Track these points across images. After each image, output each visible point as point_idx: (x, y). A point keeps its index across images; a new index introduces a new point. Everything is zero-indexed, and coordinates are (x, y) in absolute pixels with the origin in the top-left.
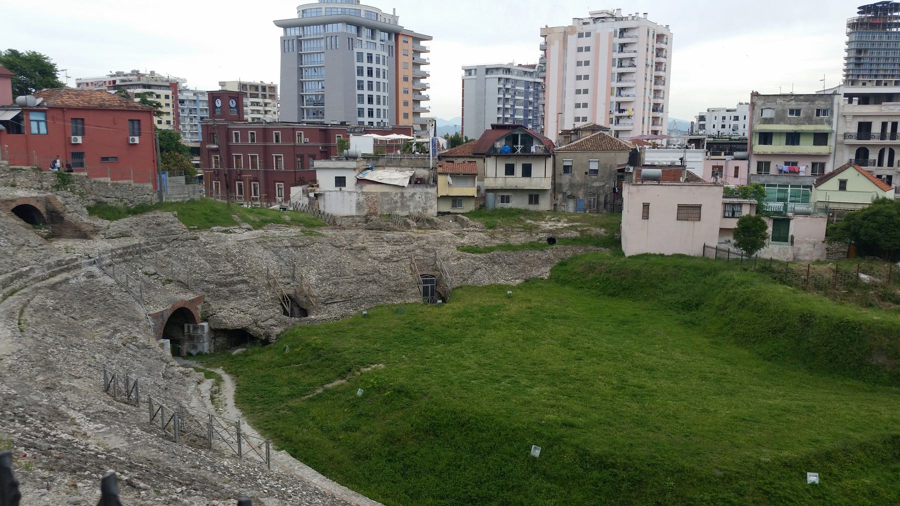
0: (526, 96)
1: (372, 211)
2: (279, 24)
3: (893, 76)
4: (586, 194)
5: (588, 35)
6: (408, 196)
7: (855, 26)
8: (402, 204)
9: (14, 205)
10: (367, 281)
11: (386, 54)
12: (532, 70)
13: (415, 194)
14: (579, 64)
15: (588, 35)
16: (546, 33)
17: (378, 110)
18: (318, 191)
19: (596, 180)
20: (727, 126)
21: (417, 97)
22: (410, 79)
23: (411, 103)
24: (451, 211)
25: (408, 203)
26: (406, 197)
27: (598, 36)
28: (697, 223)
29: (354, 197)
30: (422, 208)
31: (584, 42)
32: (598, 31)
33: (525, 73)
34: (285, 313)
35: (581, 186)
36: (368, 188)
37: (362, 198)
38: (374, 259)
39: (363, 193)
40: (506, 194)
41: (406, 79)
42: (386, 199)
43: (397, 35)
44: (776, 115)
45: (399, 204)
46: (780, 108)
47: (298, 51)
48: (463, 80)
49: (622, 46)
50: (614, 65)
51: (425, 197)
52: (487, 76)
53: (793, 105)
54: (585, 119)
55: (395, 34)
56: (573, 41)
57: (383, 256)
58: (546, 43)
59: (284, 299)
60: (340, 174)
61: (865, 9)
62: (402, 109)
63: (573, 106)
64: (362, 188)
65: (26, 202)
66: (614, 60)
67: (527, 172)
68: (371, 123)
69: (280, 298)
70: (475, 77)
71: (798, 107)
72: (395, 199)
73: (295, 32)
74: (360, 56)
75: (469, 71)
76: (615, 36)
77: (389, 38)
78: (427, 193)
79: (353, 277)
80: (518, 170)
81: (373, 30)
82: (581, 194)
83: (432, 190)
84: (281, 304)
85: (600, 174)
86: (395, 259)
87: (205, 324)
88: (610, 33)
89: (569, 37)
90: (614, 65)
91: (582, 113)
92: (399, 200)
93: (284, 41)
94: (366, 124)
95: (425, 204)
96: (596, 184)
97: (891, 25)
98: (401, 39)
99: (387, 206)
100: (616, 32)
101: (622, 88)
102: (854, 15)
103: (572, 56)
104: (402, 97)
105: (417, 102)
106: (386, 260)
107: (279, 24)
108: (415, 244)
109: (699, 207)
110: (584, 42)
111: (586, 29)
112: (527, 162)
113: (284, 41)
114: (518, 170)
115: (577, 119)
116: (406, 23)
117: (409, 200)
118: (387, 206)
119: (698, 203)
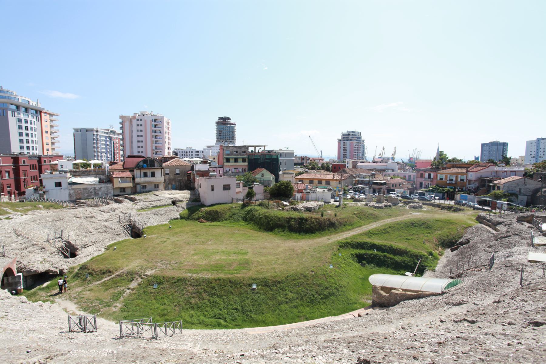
0: (106, 142)
1: (78, 197)
3: (230, 139)
4: (175, 182)
5: (141, 120)
6: (98, 188)
7: (218, 123)
8: (95, 193)
11: (35, 120)
12: (107, 131)
13: (101, 187)
14: (138, 131)
15: (141, 120)
16: (122, 117)
17: (33, 147)
18: (44, 190)
19: (179, 177)
20: (184, 155)
21: (53, 141)
22: (49, 133)
23: (50, 144)
24: (120, 194)
26: (96, 190)
27: (145, 121)
28: (229, 191)
29: (67, 192)
30: (106, 194)
31: (140, 123)
32: (145, 119)
33: (105, 132)
34: (66, 257)
35: (173, 180)
36: (74, 187)
37: (72, 192)
38: (100, 221)
39: (72, 189)
40: (144, 185)
41: (47, 132)
42: (86, 191)
43: (41, 112)
44: (231, 153)
45: (93, 193)
46: (231, 150)
48: (74, 134)
49: (156, 126)
50: (153, 132)
51: (107, 189)
52: (87, 133)
53: (235, 149)
54: (142, 152)
55: (38, 112)
56: (135, 122)
57: (104, 219)
58: (122, 122)
59: (63, 249)
61: (220, 118)
62: (46, 147)
63: (137, 147)
64: (72, 186)
66: (153, 130)
67: (153, 175)
68: (29, 153)
69: (61, 250)
70: (81, 133)
71: (237, 150)
72: (91, 191)
74: (20, 120)
75: (77, 130)
76: (153, 121)
78: (108, 187)
80: (149, 174)
81: (27, 110)
82: (173, 183)
83: (110, 185)
84: (62, 253)
85: (180, 175)
86: (111, 219)
87: (21, 274)
88: (150, 120)
89: (133, 120)
90: (153, 132)
91: (141, 150)
92: (93, 191)
94: (26, 153)
95: (107, 192)
96: (179, 179)
97: (228, 124)
98: (43, 114)
99: (87, 195)
100: (153, 120)
101: (157, 141)
102: (217, 120)
103: (135, 128)
104: (45, 141)
105: (53, 144)
106: (107, 221)
109: (229, 185)
110: (140, 123)
111: (139, 118)
112: (152, 170)
114: (149, 174)
115: (139, 152)
116: (46, 108)
117: (98, 191)
118: (87, 195)
119: (229, 184)
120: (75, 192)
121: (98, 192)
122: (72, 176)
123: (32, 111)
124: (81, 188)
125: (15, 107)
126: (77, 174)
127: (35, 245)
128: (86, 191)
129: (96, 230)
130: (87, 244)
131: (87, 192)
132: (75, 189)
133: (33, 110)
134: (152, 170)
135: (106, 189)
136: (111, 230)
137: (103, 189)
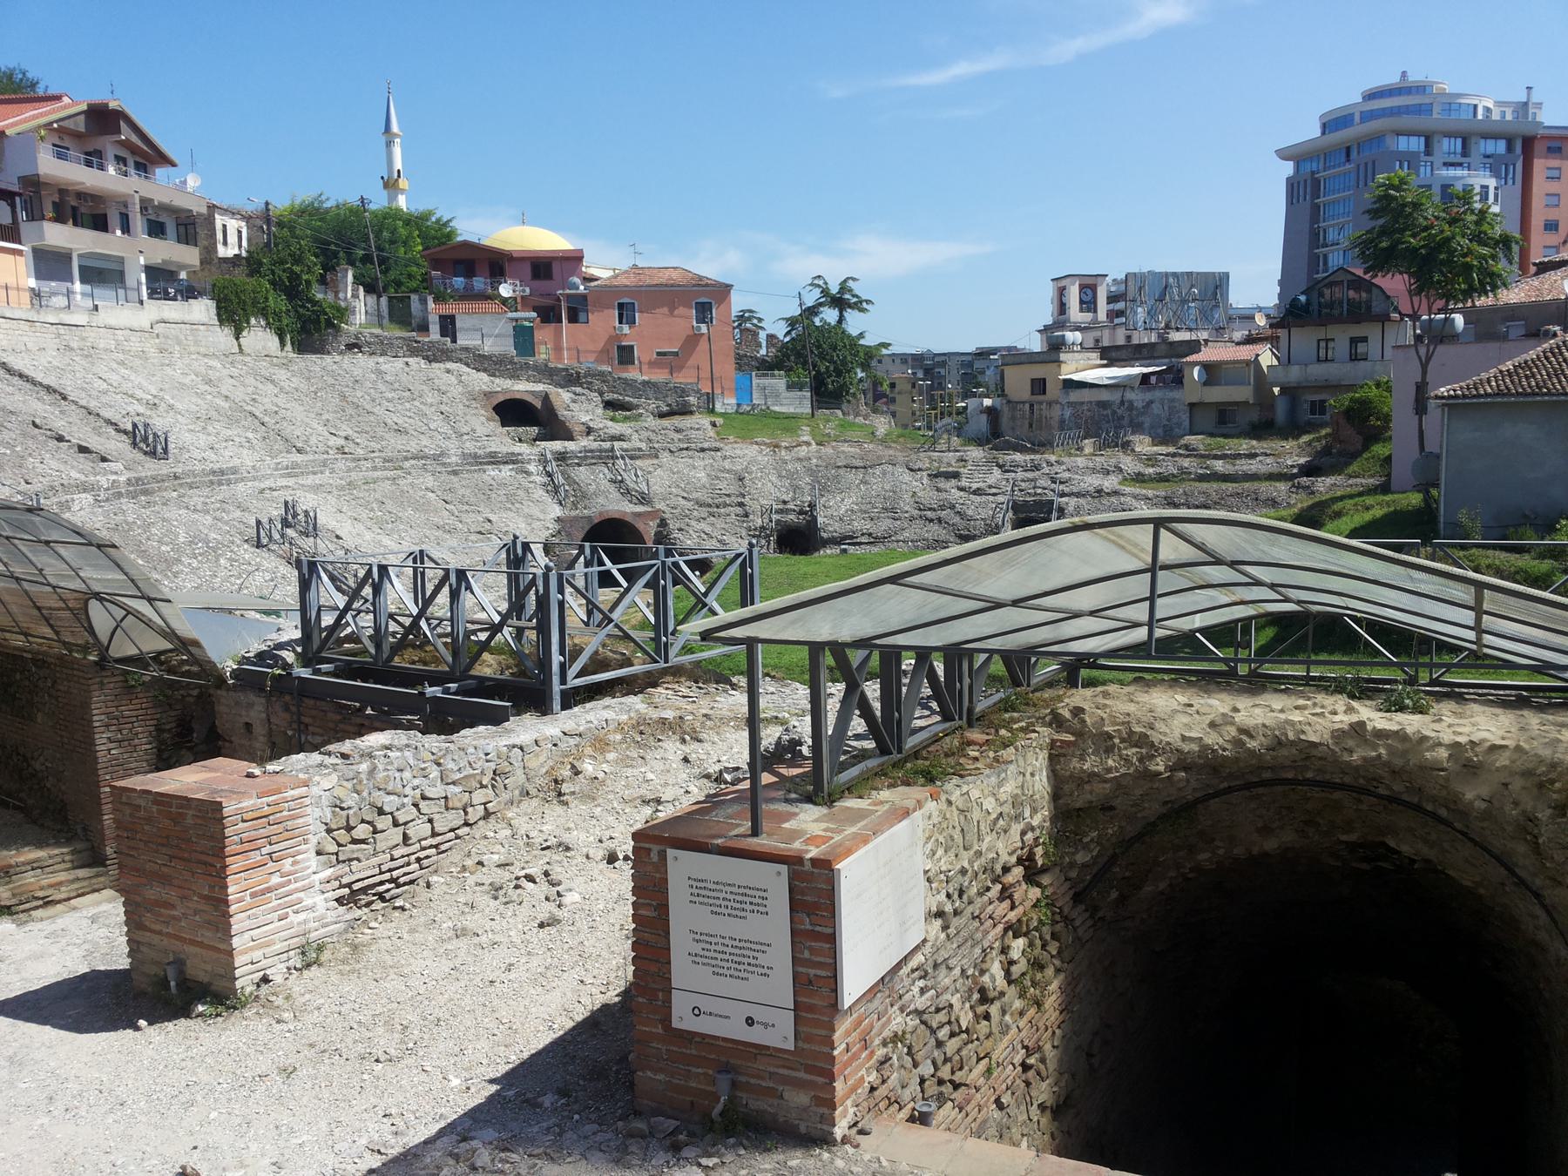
2: (1284, 154)
9: (501, 398)
10: (927, 519)
13: (1152, 402)
25: (1141, 419)
26: (1137, 409)
36: (1075, 396)
39: (1070, 404)
40: (1317, 397)
42: (1105, 413)
47: (1312, 200)
51: (1169, 408)
57: (975, 486)
60: (1038, 371)
64: (1067, 394)
65: (518, 397)
73: (1308, 167)
77: (1510, 148)
78: (1173, 400)
79: (907, 512)
80: (1341, 346)
86: (994, 491)
93: (1292, 185)
95: (1169, 420)
106: (978, 492)
107: (1284, 154)
108: (1046, 470)
113: (1292, 185)
117: (1143, 414)
120: (1076, 416)
121: (1141, 419)
122: (1105, 362)
123: (1491, 143)
124: (1091, 402)
125: (1416, 144)
126: (1124, 357)
127: (741, 505)
128: (1105, 413)
129: (920, 510)
130: (852, 537)
131: (1107, 415)
132: (1076, 403)
133: (1495, 137)
134: (1357, 330)
135: (1166, 408)
136: (957, 519)
137: (1156, 408)
